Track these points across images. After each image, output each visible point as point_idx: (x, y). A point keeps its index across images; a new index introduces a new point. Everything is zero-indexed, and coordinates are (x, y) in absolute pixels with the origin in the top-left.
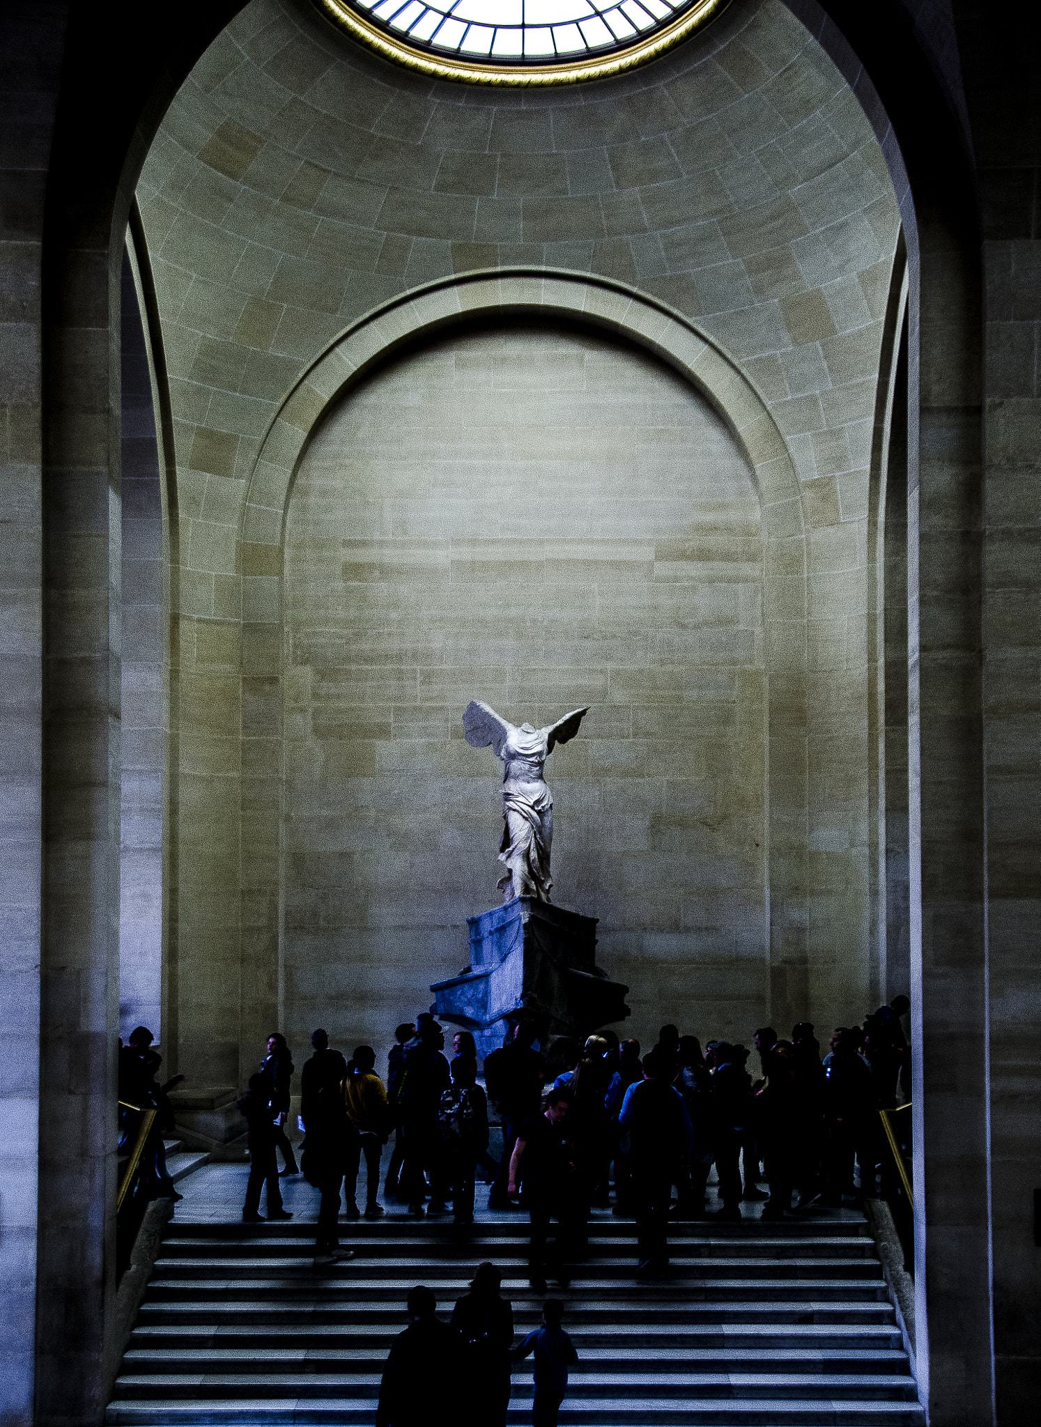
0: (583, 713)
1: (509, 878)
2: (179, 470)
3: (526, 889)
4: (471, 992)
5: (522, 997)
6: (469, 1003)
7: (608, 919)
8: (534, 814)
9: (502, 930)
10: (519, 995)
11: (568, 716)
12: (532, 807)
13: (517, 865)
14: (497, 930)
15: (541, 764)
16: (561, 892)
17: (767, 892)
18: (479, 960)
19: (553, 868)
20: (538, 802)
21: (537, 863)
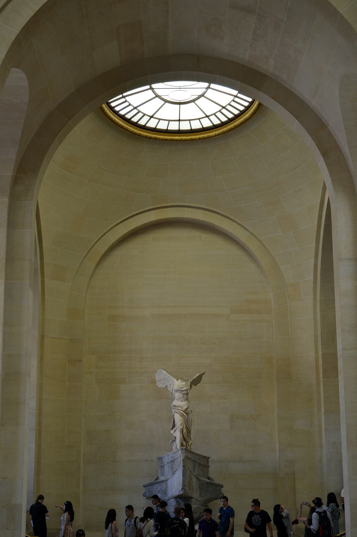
0: (204, 374)
1: (175, 440)
2: (46, 280)
3: (182, 445)
4: (160, 487)
5: (182, 489)
6: (159, 492)
7: (213, 457)
8: (185, 414)
9: (172, 461)
10: (180, 489)
11: (198, 375)
12: (184, 412)
13: (178, 435)
14: (171, 462)
15: (187, 394)
16: (199, 447)
17: (277, 446)
18: (162, 475)
19: (192, 436)
20: (186, 409)
21: (186, 434)
